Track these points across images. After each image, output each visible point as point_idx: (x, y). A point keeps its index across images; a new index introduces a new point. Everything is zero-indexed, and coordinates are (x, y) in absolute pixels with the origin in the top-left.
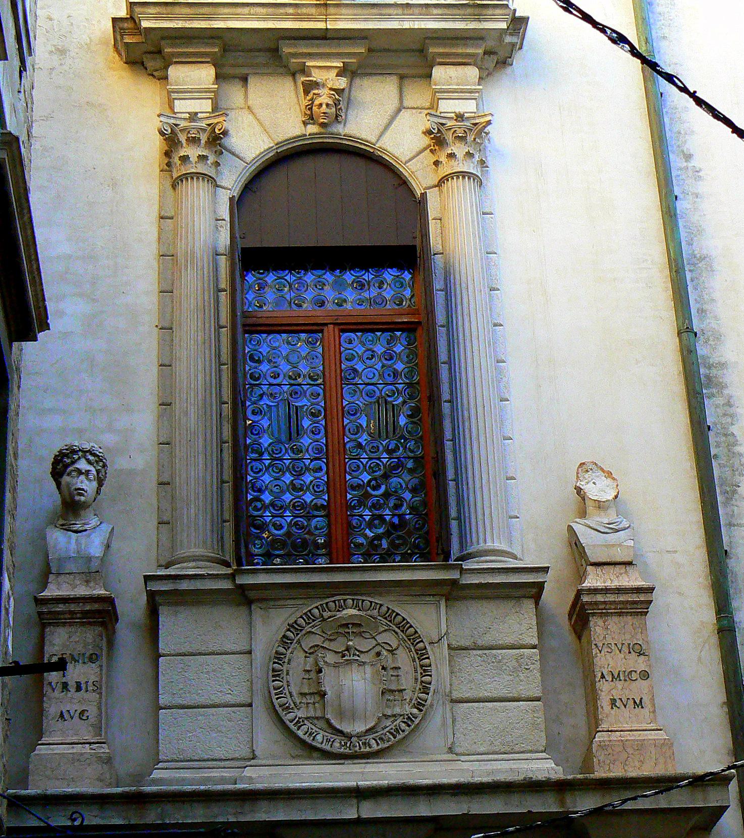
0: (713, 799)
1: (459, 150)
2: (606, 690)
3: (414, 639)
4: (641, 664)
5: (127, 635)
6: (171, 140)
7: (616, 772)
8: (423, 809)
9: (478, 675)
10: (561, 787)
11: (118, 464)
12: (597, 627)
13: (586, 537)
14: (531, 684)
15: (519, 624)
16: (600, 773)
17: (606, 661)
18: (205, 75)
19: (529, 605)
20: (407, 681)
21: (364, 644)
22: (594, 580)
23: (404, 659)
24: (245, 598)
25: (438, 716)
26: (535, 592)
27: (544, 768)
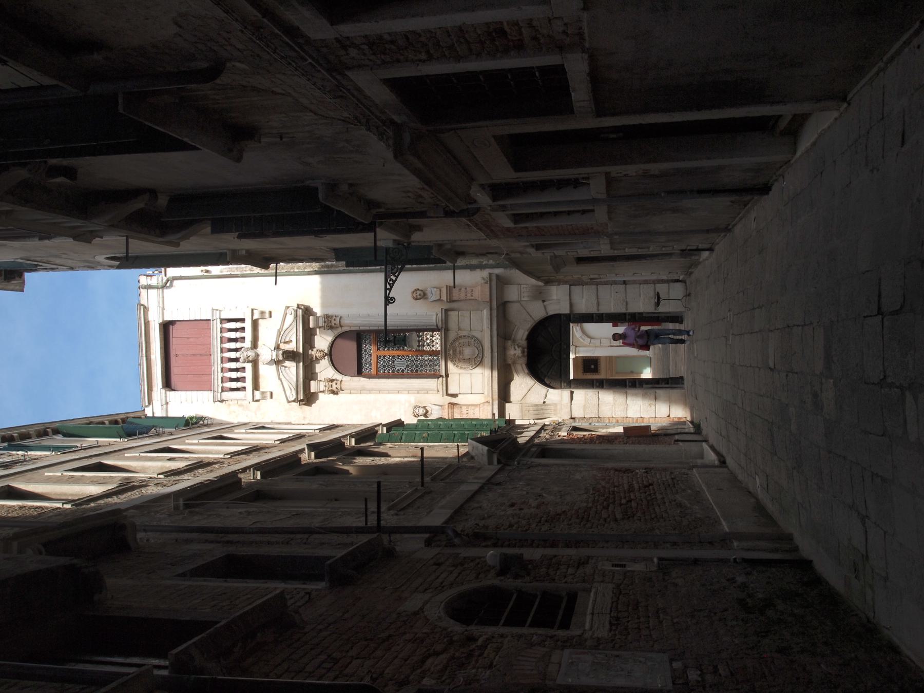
0: (494, 278)
1: (333, 322)
2: (469, 297)
3: (457, 339)
4: (463, 289)
5: (453, 400)
6: (333, 392)
7: (488, 296)
8: (495, 339)
9: (465, 324)
10: (491, 309)
11: (413, 403)
12: (454, 298)
13: (433, 298)
14: (467, 314)
15: (453, 315)
16: (488, 300)
17: (462, 296)
18: (312, 383)
19: (451, 313)
20: (466, 340)
21: (458, 349)
22: (444, 298)
23: (461, 341)
24: (447, 375)
25: (475, 334)
26: (447, 311)
27: (486, 313)
